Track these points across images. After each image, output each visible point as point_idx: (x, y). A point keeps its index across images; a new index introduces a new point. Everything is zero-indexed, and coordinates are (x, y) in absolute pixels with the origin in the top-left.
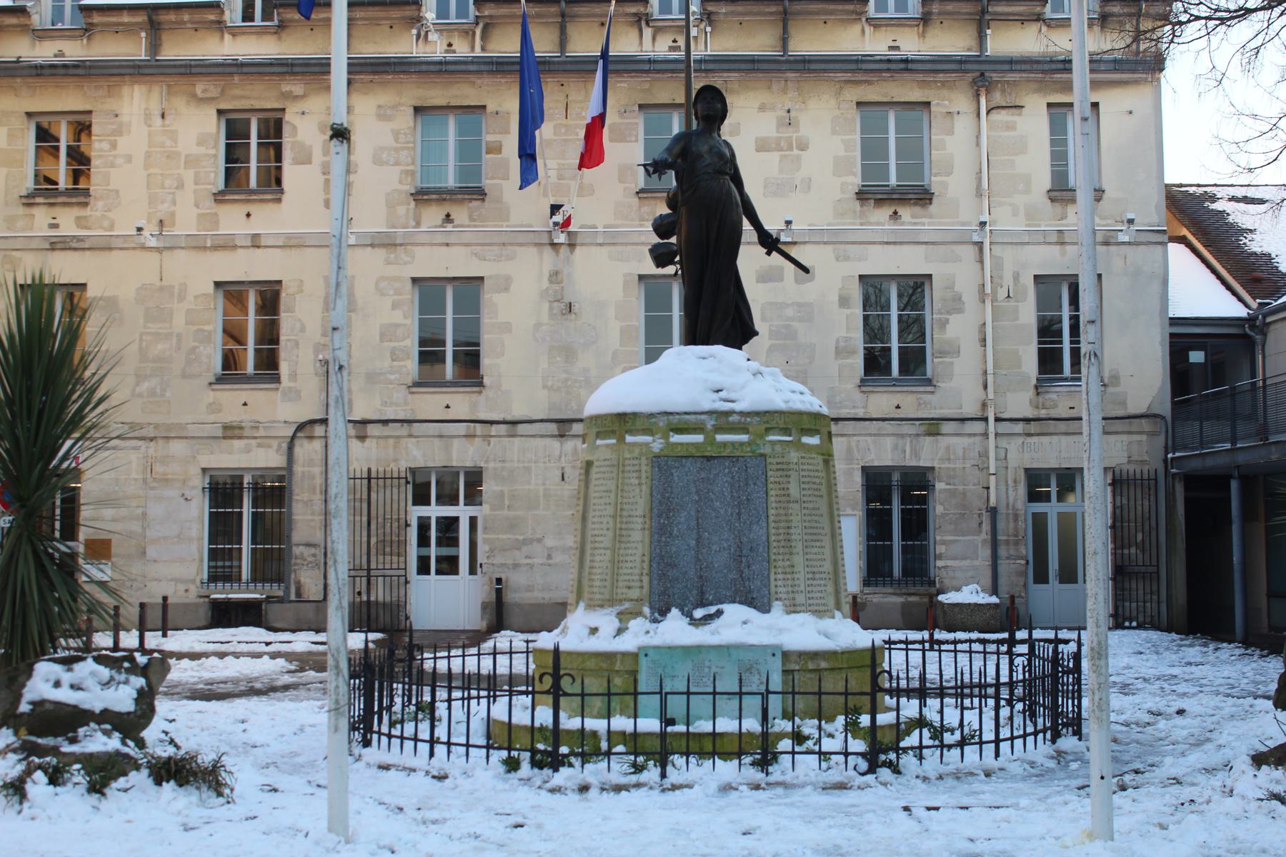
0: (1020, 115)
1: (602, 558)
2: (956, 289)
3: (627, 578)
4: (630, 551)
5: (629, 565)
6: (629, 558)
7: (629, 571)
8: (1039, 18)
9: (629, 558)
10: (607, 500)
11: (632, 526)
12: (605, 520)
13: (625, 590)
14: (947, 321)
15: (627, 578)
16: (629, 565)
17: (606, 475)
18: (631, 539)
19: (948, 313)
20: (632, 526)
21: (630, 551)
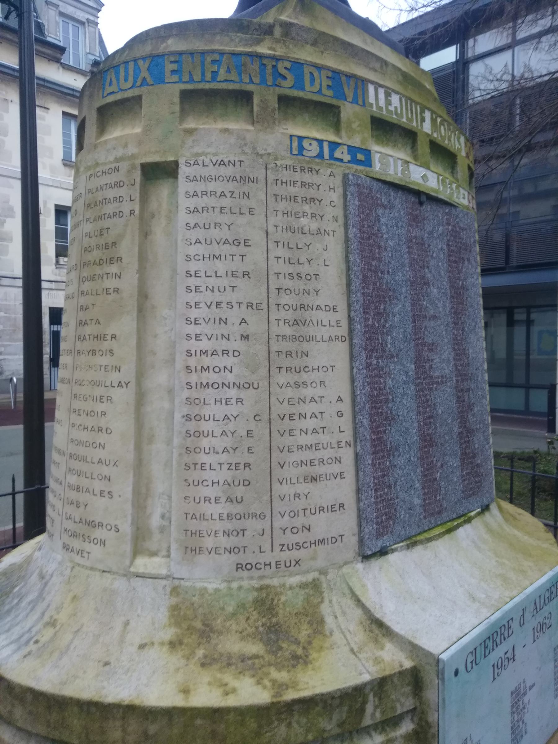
0: (47, 113)
1: (233, 410)
2: (10, 203)
3: (307, 455)
4: (309, 392)
5: (310, 424)
6: (309, 408)
7: (309, 439)
8: (58, 61)
9: (309, 408)
10: (237, 265)
11: (311, 331)
12: (233, 316)
13: (302, 488)
14: (5, 221)
15: (307, 455)
16: (310, 424)
17: (226, 202)
18: (312, 362)
19: (6, 216)
20: (311, 331)
21: (309, 392)
